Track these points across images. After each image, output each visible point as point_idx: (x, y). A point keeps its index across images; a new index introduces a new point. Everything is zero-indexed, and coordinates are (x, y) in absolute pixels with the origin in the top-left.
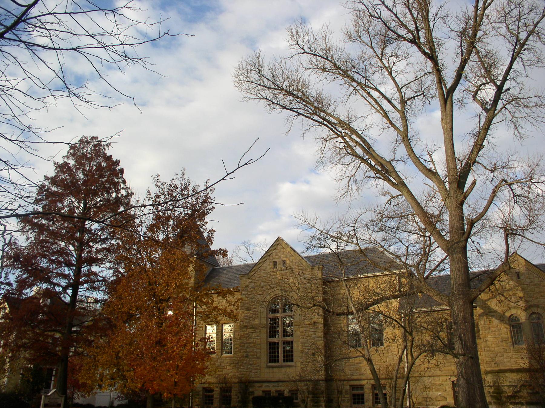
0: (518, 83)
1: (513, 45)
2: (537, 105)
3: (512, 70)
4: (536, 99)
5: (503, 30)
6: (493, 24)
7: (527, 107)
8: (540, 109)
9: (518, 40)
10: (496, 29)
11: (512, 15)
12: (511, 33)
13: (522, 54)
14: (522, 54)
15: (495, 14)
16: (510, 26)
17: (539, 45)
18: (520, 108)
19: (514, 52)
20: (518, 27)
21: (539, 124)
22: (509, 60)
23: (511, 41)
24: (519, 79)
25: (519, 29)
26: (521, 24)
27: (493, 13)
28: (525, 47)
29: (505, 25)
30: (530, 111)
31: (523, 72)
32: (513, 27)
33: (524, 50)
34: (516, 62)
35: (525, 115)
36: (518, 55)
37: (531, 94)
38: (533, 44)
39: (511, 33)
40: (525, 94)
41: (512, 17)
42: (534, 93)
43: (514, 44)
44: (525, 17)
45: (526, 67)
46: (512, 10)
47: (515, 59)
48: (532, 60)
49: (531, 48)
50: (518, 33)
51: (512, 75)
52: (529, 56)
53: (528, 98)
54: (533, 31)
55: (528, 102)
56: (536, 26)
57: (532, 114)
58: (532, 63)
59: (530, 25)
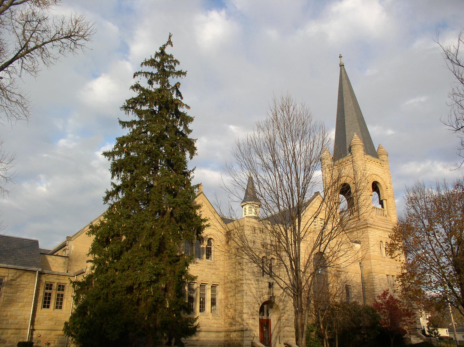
0: (11, 78)
1: (21, 47)
2: (17, 102)
3: (11, 65)
4: (18, 97)
5: (19, 31)
6: (14, 21)
7: (9, 100)
8: (18, 106)
9: (26, 46)
10: (15, 27)
11: (32, 24)
12: (25, 38)
13: (25, 58)
14: (25, 58)
15: (19, 14)
16: (26, 31)
17: (39, 59)
18: (3, 98)
19: (19, 53)
20: (31, 36)
21: (12, 117)
22: (12, 56)
23: (22, 43)
24: (13, 76)
25: (31, 38)
26: (34, 35)
27: (18, 12)
28: (29, 54)
29: (23, 28)
30: (10, 104)
31: (19, 72)
32: (28, 34)
33: (28, 56)
34: (17, 61)
35: (5, 105)
36: (21, 57)
37: (16, 92)
38: (35, 55)
39: (25, 38)
40: (12, 89)
41: (31, 26)
42: (19, 93)
43: (23, 47)
44: (40, 32)
45: (23, 69)
46: (33, 21)
47: (18, 58)
48: (30, 67)
49: (33, 58)
50: (29, 41)
51: (9, 68)
52: (29, 63)
53: (13, 93)
54: (40, 46)
55: (12, 96)
56: (44, 44)
57: (10, 107)
58: (28, 69)
59: (39, 41)
